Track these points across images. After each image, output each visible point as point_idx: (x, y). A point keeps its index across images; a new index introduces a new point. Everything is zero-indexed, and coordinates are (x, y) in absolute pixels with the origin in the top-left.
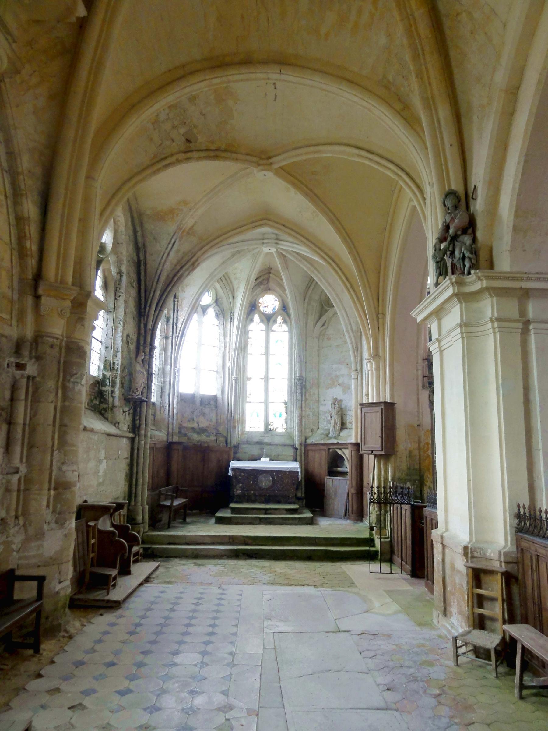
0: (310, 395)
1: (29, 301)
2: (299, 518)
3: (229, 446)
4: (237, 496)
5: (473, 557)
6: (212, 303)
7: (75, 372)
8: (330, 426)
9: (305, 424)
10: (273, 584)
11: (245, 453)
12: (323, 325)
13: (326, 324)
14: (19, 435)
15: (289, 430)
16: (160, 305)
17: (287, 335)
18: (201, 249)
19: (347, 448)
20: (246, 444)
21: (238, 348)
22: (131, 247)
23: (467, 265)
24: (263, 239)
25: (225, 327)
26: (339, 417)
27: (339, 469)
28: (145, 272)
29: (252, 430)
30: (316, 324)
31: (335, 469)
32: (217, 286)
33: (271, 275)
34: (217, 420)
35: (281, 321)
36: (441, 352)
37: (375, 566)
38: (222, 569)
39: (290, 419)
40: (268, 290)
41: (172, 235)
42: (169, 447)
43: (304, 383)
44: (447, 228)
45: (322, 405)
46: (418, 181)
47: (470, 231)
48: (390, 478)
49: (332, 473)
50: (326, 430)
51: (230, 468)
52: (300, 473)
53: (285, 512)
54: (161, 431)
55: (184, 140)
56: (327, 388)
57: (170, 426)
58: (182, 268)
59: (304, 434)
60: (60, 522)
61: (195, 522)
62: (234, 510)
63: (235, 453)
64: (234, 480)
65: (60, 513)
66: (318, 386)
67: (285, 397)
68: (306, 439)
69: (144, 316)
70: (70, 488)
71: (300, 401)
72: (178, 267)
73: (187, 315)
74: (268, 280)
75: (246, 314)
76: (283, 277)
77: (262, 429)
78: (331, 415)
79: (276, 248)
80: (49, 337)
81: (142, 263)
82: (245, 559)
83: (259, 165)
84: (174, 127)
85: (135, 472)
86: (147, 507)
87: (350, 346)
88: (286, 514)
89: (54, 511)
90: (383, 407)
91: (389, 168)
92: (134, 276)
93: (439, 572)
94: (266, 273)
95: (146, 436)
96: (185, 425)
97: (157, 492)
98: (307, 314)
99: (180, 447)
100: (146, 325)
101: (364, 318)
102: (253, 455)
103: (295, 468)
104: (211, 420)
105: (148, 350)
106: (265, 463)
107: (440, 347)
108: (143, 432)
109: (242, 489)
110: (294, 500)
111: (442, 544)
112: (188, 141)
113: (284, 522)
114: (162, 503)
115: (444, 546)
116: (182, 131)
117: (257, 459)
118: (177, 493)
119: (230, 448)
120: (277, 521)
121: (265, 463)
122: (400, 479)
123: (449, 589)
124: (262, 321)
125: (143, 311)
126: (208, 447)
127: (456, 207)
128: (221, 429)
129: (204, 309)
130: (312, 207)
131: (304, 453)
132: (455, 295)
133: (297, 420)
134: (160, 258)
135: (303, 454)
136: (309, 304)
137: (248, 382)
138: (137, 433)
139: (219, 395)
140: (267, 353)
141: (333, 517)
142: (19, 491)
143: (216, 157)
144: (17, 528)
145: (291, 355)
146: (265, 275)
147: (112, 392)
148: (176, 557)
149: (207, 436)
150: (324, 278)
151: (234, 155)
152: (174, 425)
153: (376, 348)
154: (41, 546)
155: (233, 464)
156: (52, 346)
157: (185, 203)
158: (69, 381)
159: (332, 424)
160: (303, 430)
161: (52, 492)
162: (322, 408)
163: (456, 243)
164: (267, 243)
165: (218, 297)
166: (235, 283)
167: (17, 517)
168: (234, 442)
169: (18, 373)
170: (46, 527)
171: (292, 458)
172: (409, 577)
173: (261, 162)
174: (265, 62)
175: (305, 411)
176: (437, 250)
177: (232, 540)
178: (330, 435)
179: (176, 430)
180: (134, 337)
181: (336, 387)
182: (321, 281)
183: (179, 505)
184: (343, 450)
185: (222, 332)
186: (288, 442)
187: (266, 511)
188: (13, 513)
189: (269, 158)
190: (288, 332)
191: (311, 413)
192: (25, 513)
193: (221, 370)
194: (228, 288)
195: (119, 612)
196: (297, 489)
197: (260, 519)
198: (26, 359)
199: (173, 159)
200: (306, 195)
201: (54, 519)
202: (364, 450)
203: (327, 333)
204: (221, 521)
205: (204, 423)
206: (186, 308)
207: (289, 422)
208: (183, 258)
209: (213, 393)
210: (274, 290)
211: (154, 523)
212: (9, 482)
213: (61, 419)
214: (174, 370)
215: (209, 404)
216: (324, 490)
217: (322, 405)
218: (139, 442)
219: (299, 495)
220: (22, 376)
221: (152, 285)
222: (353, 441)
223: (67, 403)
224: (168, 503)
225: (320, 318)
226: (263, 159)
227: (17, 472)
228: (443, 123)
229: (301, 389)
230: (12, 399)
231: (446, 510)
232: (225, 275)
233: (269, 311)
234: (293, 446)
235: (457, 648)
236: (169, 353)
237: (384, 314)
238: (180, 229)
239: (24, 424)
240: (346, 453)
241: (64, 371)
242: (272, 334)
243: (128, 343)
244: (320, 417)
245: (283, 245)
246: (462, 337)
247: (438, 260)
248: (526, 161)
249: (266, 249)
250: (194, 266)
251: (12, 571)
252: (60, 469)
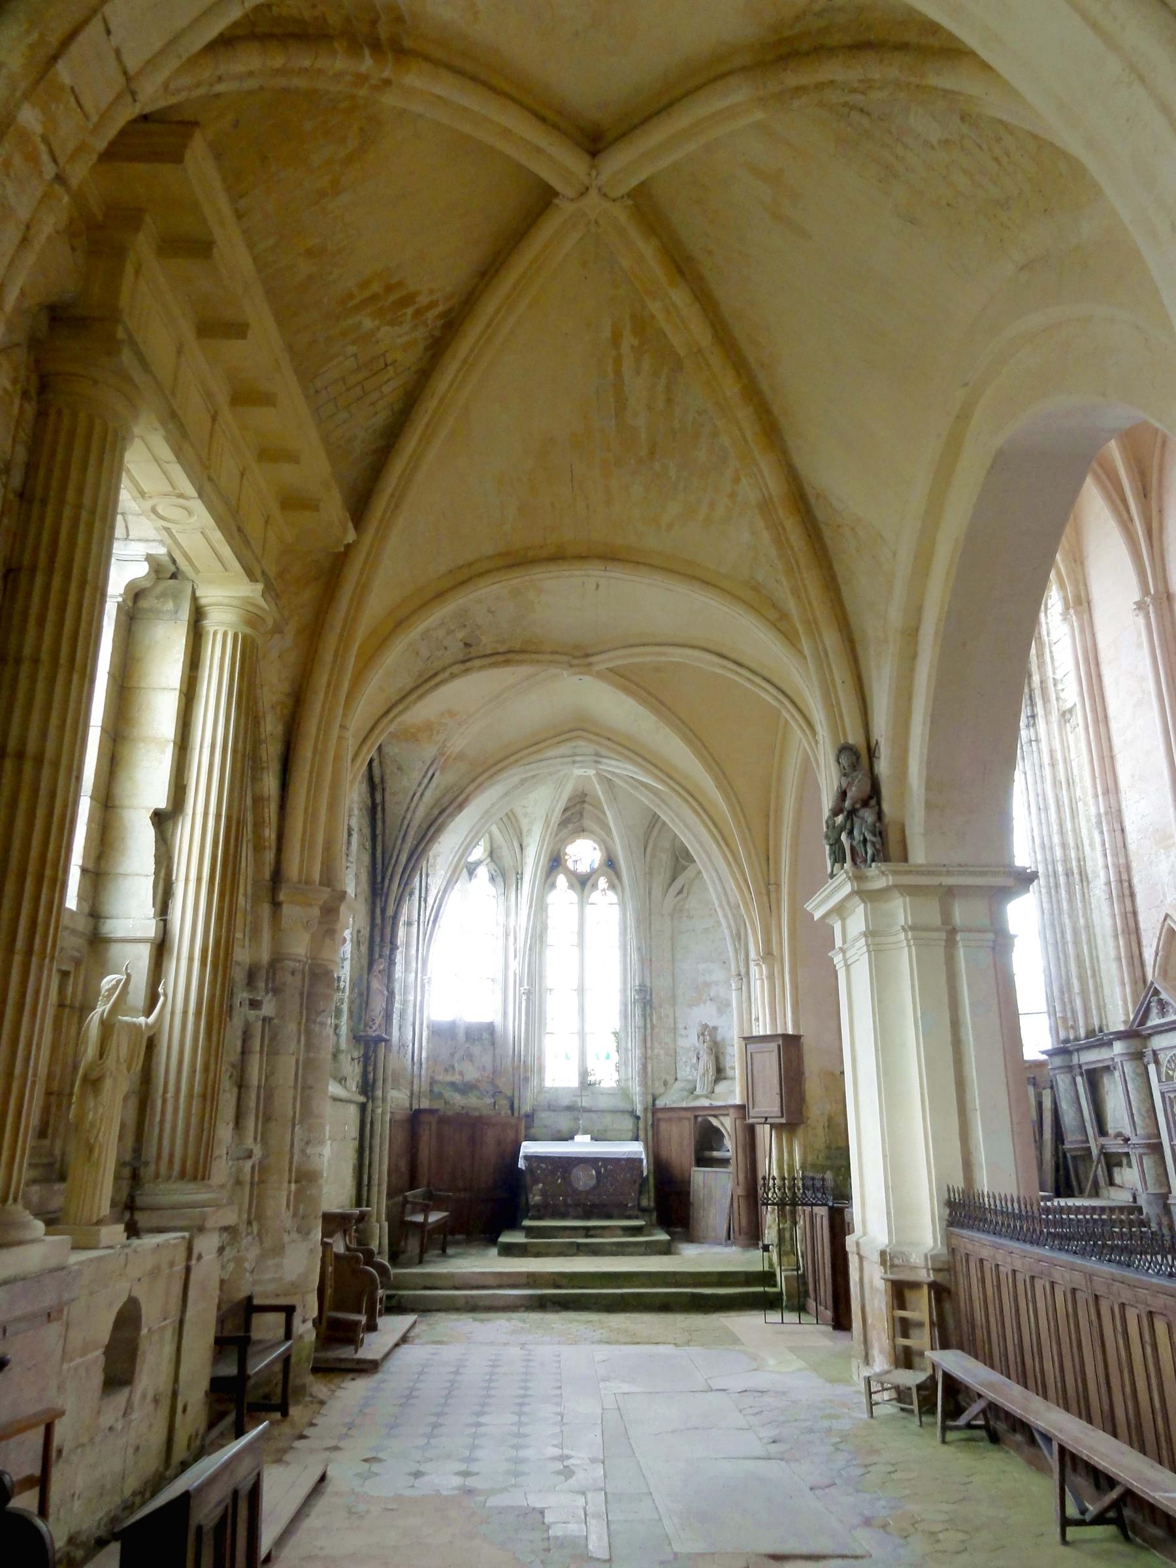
0: (660, 1018)
1: (266, 909)
2: (646, 1242)
3: (516, 1114)
4: (534, 1206)
5: (892, 1266)
6: (483, 857)
7: (322, 1008)
8: (697, 1075)
9: (652, 1072)
10: (608, 1343)
11: (546, 1127)
12: (680, 892)
13: (685, 891)
14: (252, 1104)
15: (623, 1084)
16: (406, 876)
17: (616, 911)
18: (474, 780)
19: (728, 1115)
20: (545, 1110)
21: (531, 937)
22: (364, 787)
23: (870, 852)
24: (575, 755)
25: (507, 899)
26: (713, 1057)
27: (716, 1154)
28: (384, 822)
29: (556, 1085)
30: (667, 891)
31: (707, 1154)
32: (494, 829)
33: (585, 806)
34: (494, 1067)
35: (606, 886)
36: (848, 967)
37: (774, 1317)
38: (521, 1325)
39: (626, 1064)
40: (581, 831)
41: (429, 763)
42: (414, 1120)
43: (648, 998)
44: (843, 794)
45: (681, 1036)
46: (806, 712)
47: (873, 802)
48: (798, 1165)
49: (702, 1161)
50: (689, 1081)
51: (521, 1154)
52: (645, 1162)
53: (620, 1232)
54: (399, 1090)
55: (461, 644)
56: (690, 1006)
57: (416, 1081)
58: (441, 813)
59: (650, 1091)
60: (304, 1232)
61: (462, 1254)
62: (530, 1232)
63: (528, 1127)
64: (528, 1178)
65: (303, 1218)
66: (673, 999)
67: (616, 1023)
68: (654, 1100)
69: (381, 895)
70: (316, 1181)
71: (642, 1030)
72: (436, 812)
73: (445, 883)
74: (581, 814)
75: (544, 876)
76: (608, 813)
77: (574, 1082)
78: (698, 1054)
79: (596, 769)
80: (290, 960)
81: (379, 808)
82: (557, 1312)
83: (571, 666)
84: (450, 632)
85: (367, 1163)
86: (386, 1225)
87: (726, 931)
88: (624, 1236)
89: (295, 1215)
90: (781, 1043)
91: (767, 691)
92: (367, 831)
93: (856, 1299)
94: (578, 803)
95: (384, 1100)
96: (439, 1078)
97: (400, 1199)
98: (651, 874)
99: (433, 1119)
100: (383, 911)
101: (746, 891)
102: (559, 1131)
103: (636, 1153)
104: (484, 1067)
105: (387, 952)
106: (584, 1144)
107: (845, 960)
108: (379, 1093)
109: (543, 1193)
110: (636, 1212)
111: (858, 1254)
112: (467, 645)
113: (619, 1250)
114: (409, 1219)
115: (861, 1258)
116: (460, 635)
117: (569, 1137)
118: (432, 1201)
119: (519, 1119)
120: (608, 1248)
121: (582, 1145)
122: (814, 1166)
123: (869, 1321)
124: (571, 886)
125: (379, 886)
126: (480, 1117)
127: (854, 767)
128: (503, 1084)
129: (471, 870)
130: (653, 718)
131: (653, 1125)
132: (854, 893)
133: (637, 1066)
134: (409, 799)
135: (649, 1128)
136: (653, 855)
137: (548, 995)
138: (370, 1094)
139: (498, 1021)
140: (581, 943)
141: (707, 1243)
142: (252, 1184)
143: (507, 662)
144: (250, 1238)
145: (624, 947)
146: (575, 805)
147: (337, 1027)
148: (439, 1310)
149: (478, 1098)
150: (677, 815)
151: (534, 656)
152: (423, 1079)
153: (767, 941)
154: (279, 1266)
155: (525, 1147)
156: (293, 973)
157: (452, 714)
158: (315, 1022)
159: (701, 1071)
160: (650, 1083)
161: (293, 1186)
162: (683, 1043)
163: (855, 818)
164: (580, 762)
165: (495, 846)
166: (524, 823)
167: (249, 1223)
168: (526, 1108)
170: (286, 1238)
171: (630, 1135)
172: (830, 1329)
173: (575, 662)
174: (583, 557)
175: (652, 1048)
176: (831, 827)
177: (533, 1279)
178: (698, 1091)
179: (425, 1088)
180: (366, 932)
181: (705, 1002)
182: (672, 820)
183: (437, 1221)
184: (722, 1118)
185: (502, 908)
186: (623, 1105)
187: (588, 1232)
188: (245, 1216)
189: (587, 655)
190: (617, 906)
191: (662, 1052)
192: (260, 1217)
193: (499, 977)
194: (511, 831)
195: (378, 1376)
196: (641, 1193)
197: (578, 1245)
198: (263, 993)
199: (447, 674)
200: (643, 702)
201: (296, 1226)
202: (753, 1117)
203: (687, 906)
204: (509, 1250)
205: (471, 1074)
206: (443, 872)
207: (623, 1069)
208: (443, 796)
209: (486, 1019)
210: (592, 832)
211: (394, 1257)
212: (240, 1170)
213: (304, 1080)
214: (422, 980)
215: (480, 1039)
216: (689, 1193)
217: (681, 1036)
218: (373, 1111)
219: (644, 1203)
220: (257, 1017)
221: (395, 844)
222: (738, 1102)
223: (312, 1055)
224: (420, 1218)
225: (674, 880)
226: (575, 657)
227: (250, 1157)
228: (830, 651)
229: (644, 1009)
230: (243, 1053)
231: (863, 1204)
232: (510, 814)
233: (583, 868)
234: (632, 1113)
235: (871, 1394)
236: (413, 951)
237: (778, 885)
238: (443, 754)
239: (259, 1087)
240: (726, 1125)
241: (307, 1009)
242: (588, 908)
243: (359, 943)
244: (678, 1058)
245: (606, 764)
246: (869, 951)
247: (831, 842)
248: (932, 722)
249: (578, 772)
250: (461, 807)
251: (250, 1298)
252: (303, 1152)
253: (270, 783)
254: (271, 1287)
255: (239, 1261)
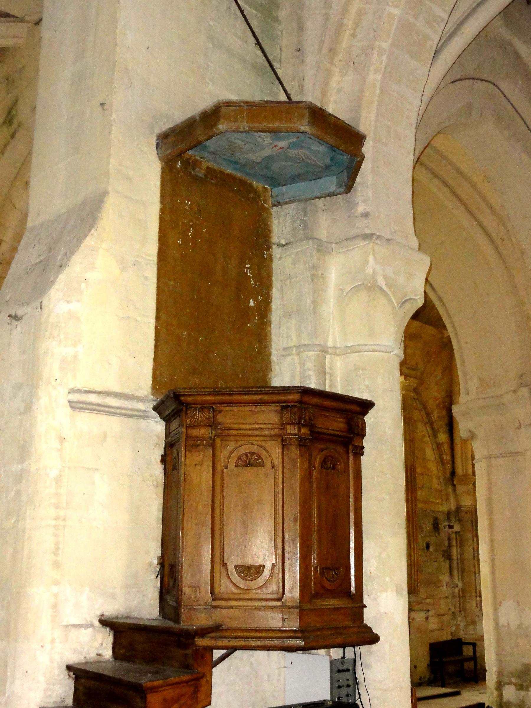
1: (450, 488)
142: (459, 597)
154: (474, 629)
167: (460, 612)
169: (450, 530)
192: (464, 610)
198: (453, 522)
212: (453, 592)
227: (457, 587)
239: (457, 559)
253: (443, 437)
254: (472, 637)
255: (458, 626)
